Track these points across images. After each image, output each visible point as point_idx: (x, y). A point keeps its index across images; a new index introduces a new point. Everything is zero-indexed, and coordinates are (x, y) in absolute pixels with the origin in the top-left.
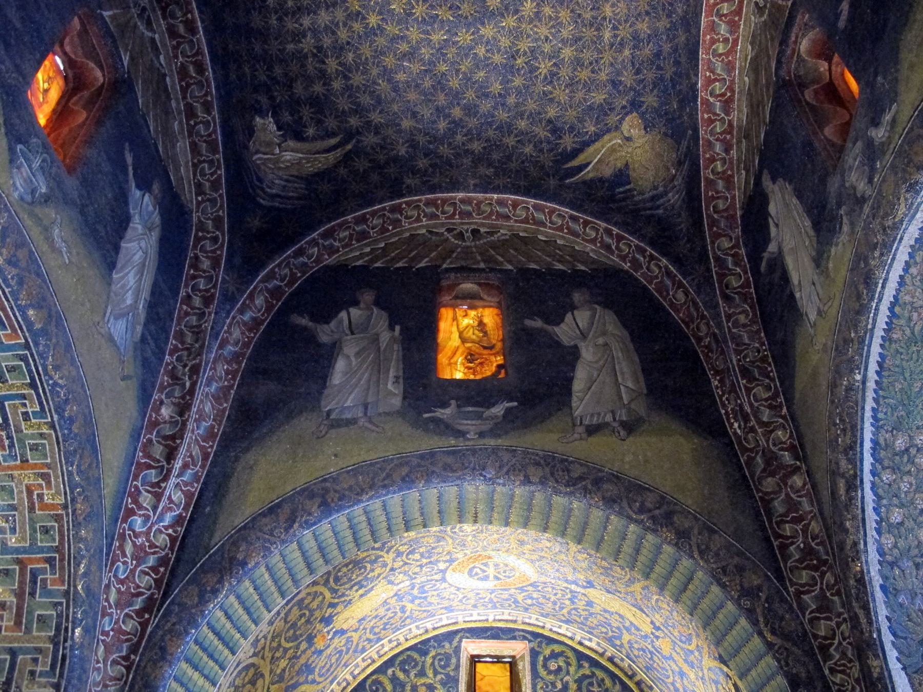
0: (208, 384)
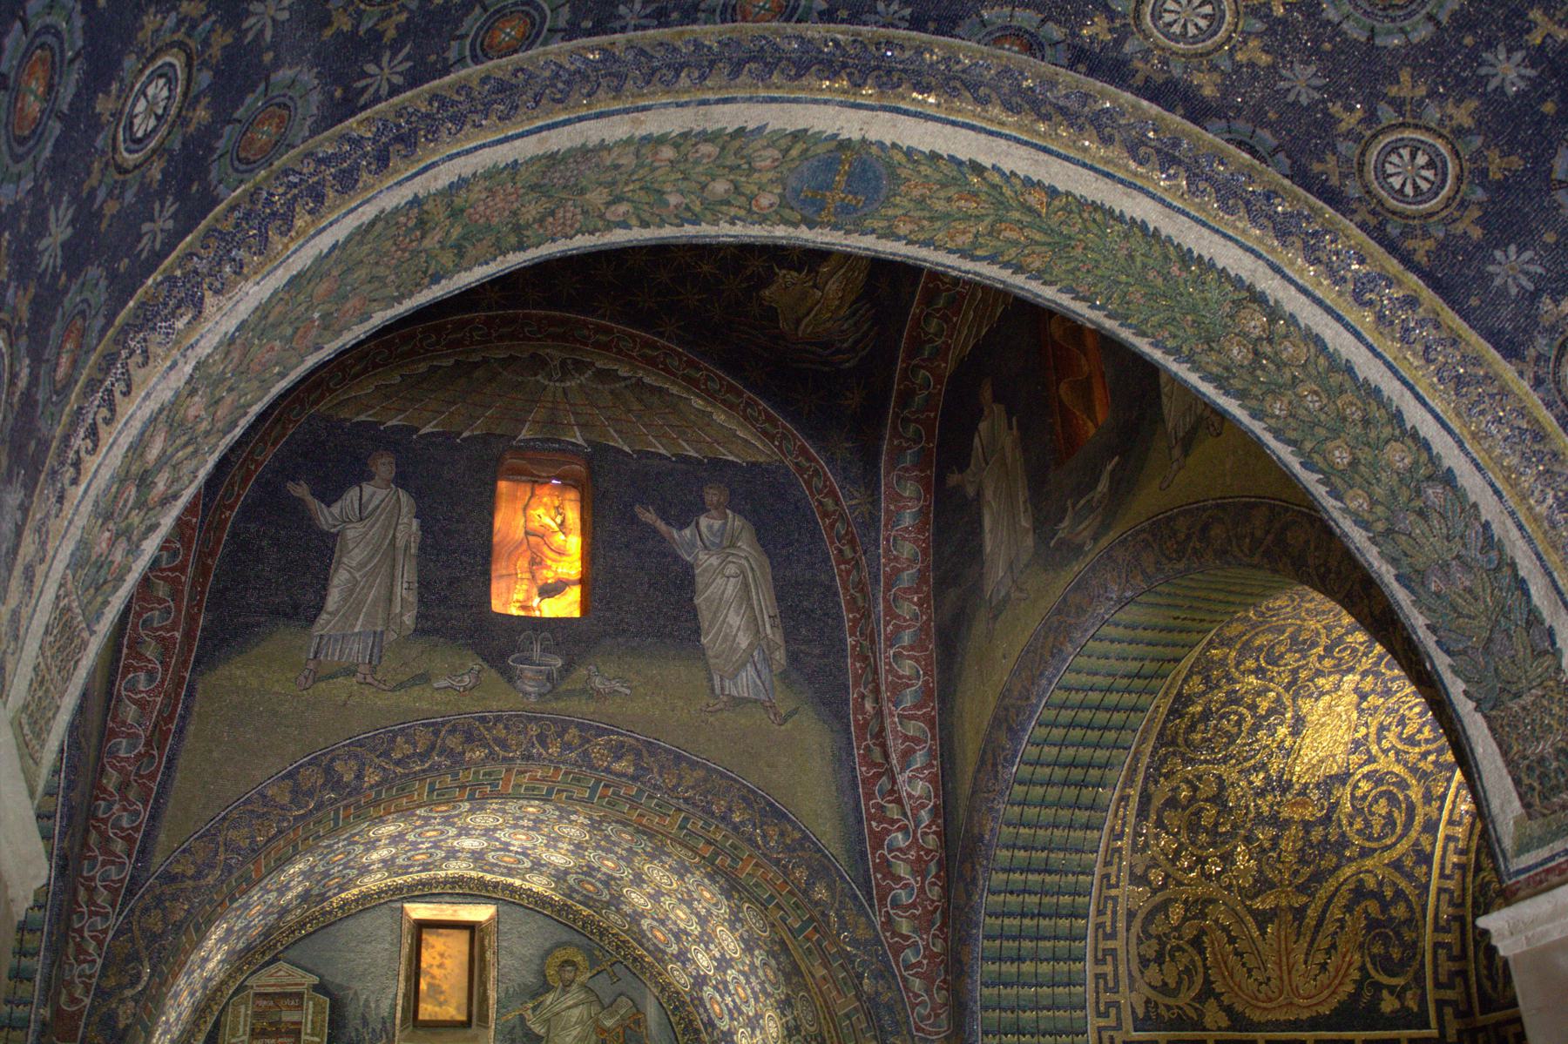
0: (892, 640)
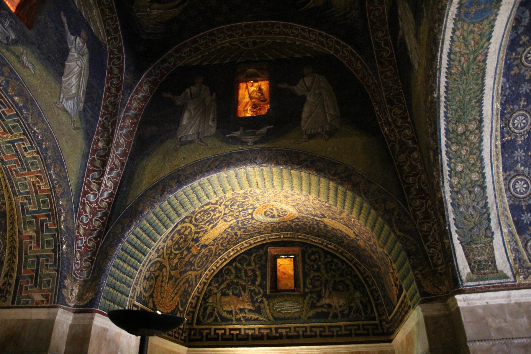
0: (122, 128)
